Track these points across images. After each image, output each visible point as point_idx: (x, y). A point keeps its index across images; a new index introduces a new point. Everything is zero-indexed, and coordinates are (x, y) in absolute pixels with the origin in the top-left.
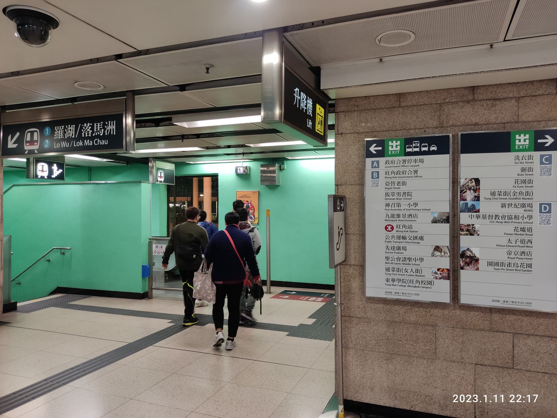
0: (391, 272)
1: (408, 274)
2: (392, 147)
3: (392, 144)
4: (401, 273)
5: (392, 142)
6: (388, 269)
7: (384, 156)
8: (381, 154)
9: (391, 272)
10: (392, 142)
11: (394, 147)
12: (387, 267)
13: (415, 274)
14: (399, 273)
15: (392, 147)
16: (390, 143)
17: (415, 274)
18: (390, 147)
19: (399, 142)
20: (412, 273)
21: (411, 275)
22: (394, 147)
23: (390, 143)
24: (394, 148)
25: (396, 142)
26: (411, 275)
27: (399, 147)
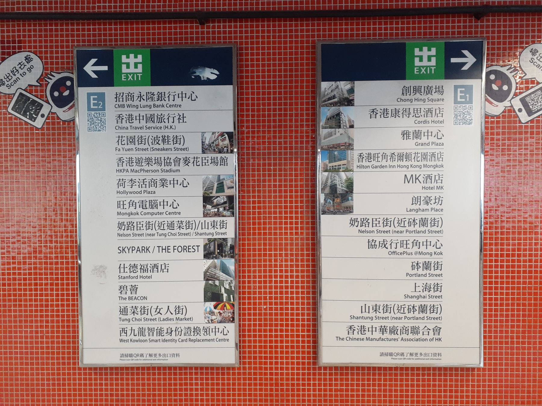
0: (130, 316)
1: (162, 317)
3: (127, 61)
4: (149, 316)
5: (128, 57)
6: (123, 311)
9: (130, 316)
10: (128, 57)
11: (132, 66)
12: (123, 306)
13: (174, 316)
14: (145, 316)
15: (128, 66)
16: (124, 58)
17: (174, 316)
18: (124, 67)
19: (140, 57)
20: (169, 315)
21: (168, 319)
22: (132, 66)
23: (124, 58)
24: (132, 70)
25: (136, 57)
26: (168, 319)
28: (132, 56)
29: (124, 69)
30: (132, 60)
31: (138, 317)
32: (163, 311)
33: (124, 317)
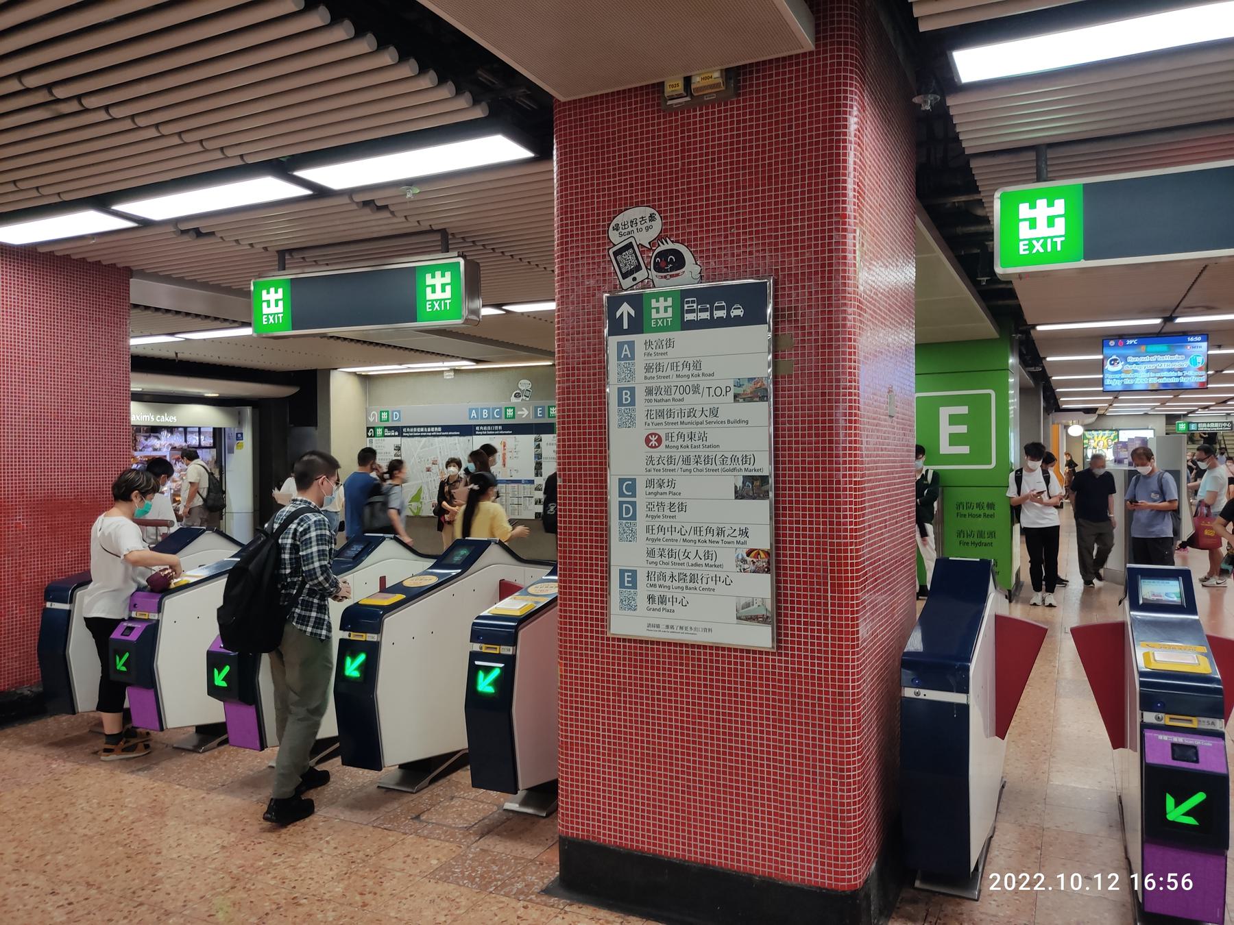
1: (691, 562)
2: (658, 312)
3: (657, 305)
4: (677, 560)
7: (641, 332)
8: (637, 325)
9: (657, 559)
11: (662, 310)
12: (650, 547)
13: (703, 562)
15: (658, 312)
18: (654, 311)
21: (696, 565)
22: (662, 310)
24: (662, 314)
26: (696, 565)
27: (670, 310)
28: (662, 299)
29: (654, 315)
30: (662, 303)
31: (666, 560)
32: (692, 555)
33: (651, 560)
